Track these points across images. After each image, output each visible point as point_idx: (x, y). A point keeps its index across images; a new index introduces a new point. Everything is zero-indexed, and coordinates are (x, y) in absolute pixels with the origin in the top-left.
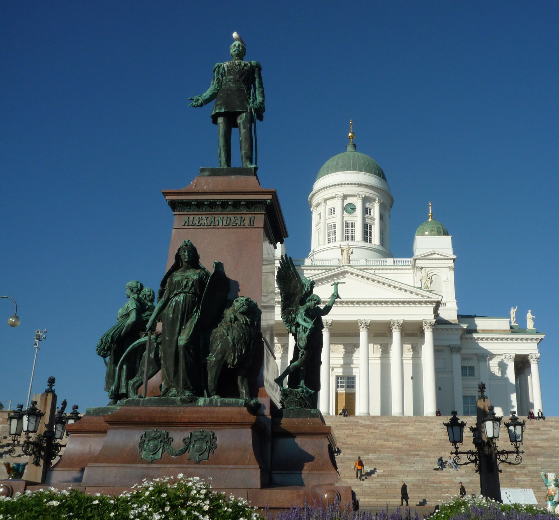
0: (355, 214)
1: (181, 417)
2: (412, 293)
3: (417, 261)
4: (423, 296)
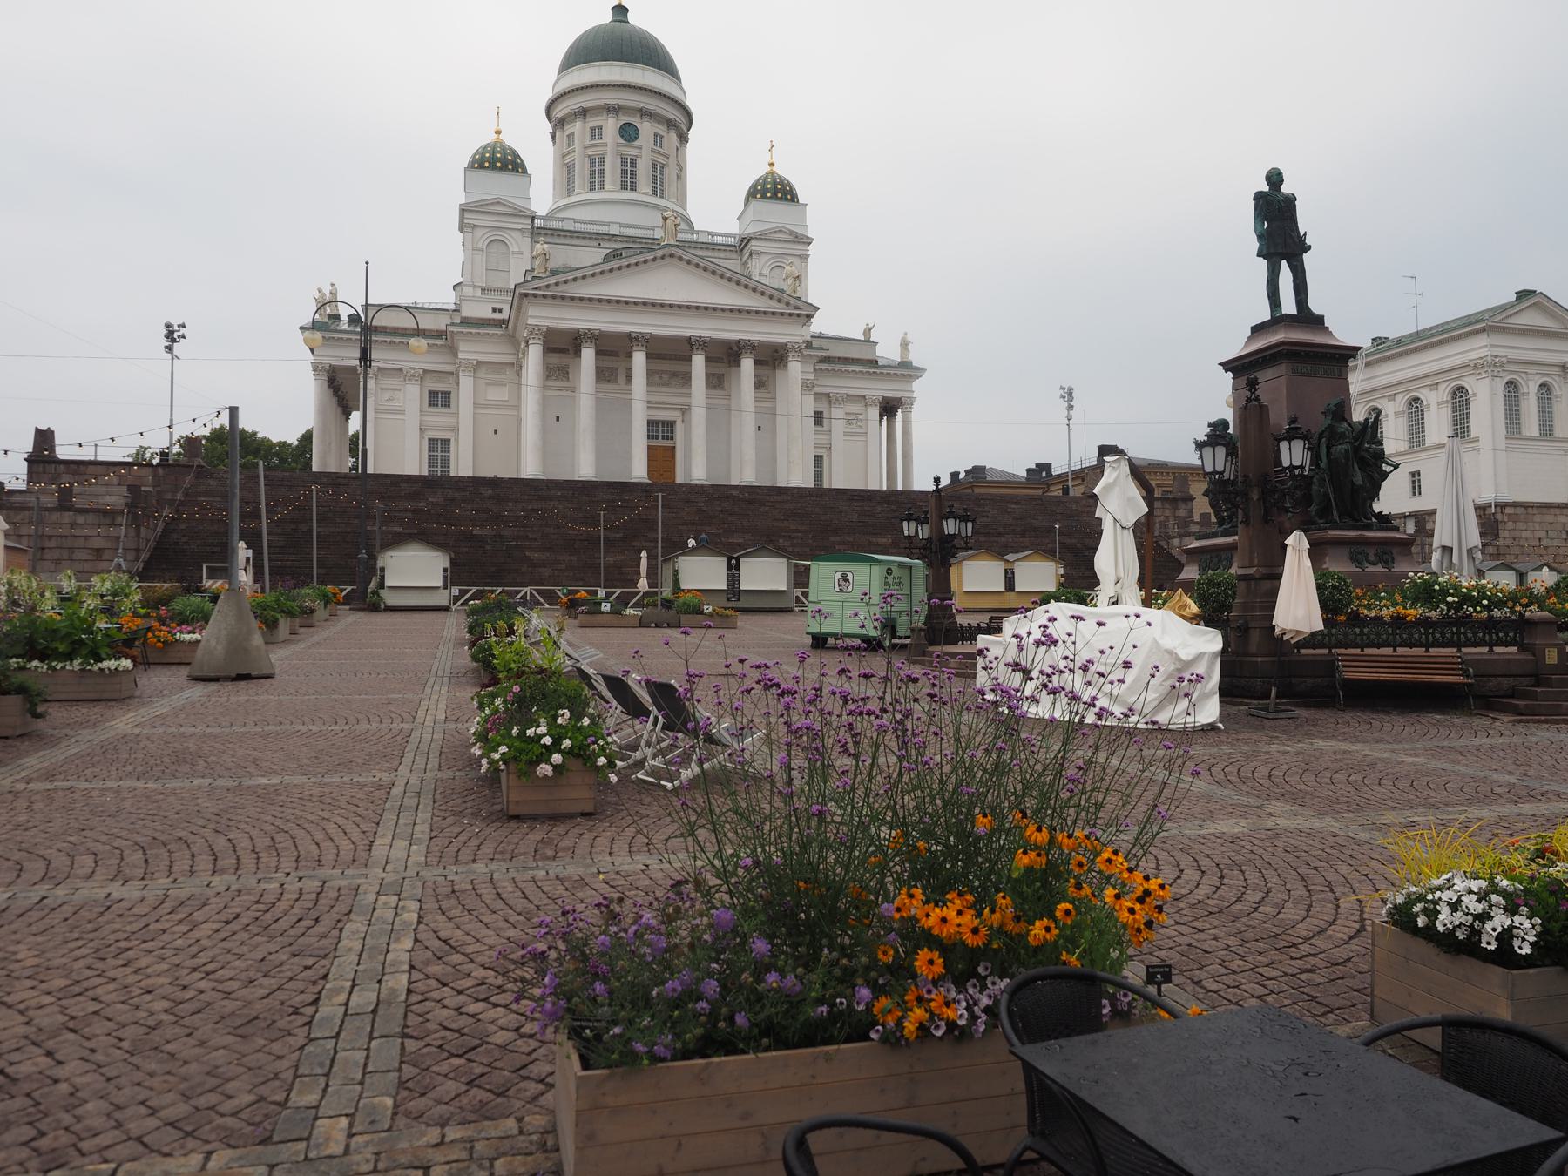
2: (771, 297)
3: (753, 242)
4: (788, 304)
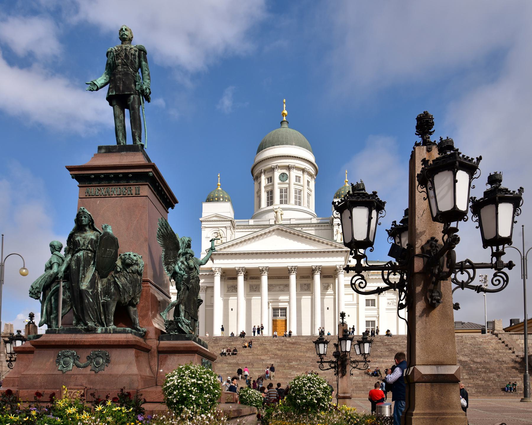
0: (287, 181)
1: (84, 341)
